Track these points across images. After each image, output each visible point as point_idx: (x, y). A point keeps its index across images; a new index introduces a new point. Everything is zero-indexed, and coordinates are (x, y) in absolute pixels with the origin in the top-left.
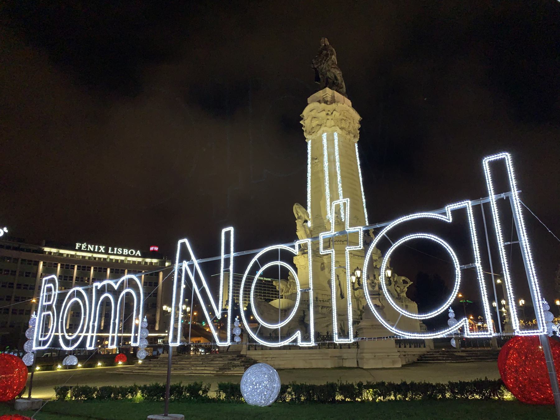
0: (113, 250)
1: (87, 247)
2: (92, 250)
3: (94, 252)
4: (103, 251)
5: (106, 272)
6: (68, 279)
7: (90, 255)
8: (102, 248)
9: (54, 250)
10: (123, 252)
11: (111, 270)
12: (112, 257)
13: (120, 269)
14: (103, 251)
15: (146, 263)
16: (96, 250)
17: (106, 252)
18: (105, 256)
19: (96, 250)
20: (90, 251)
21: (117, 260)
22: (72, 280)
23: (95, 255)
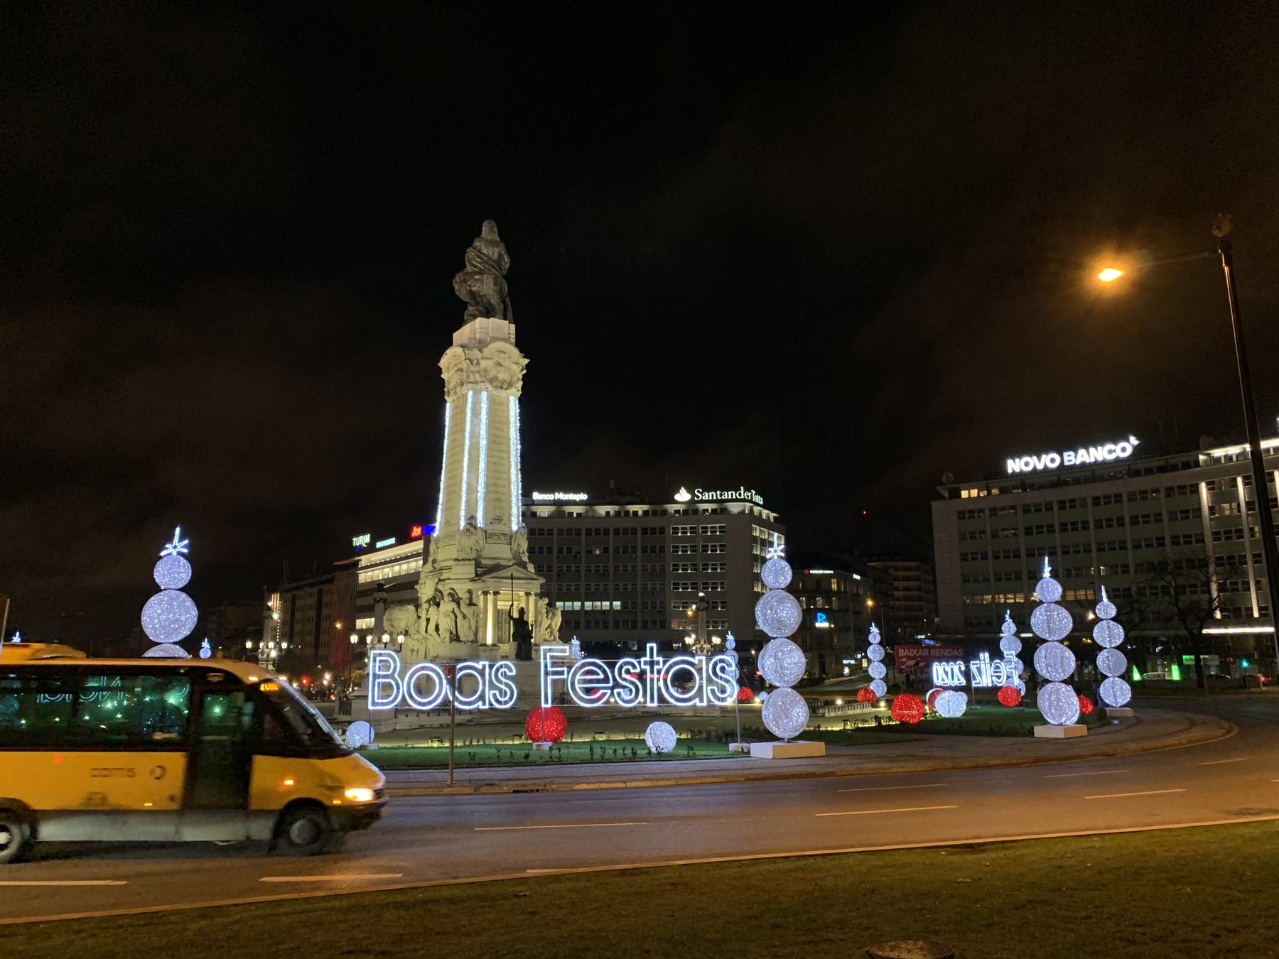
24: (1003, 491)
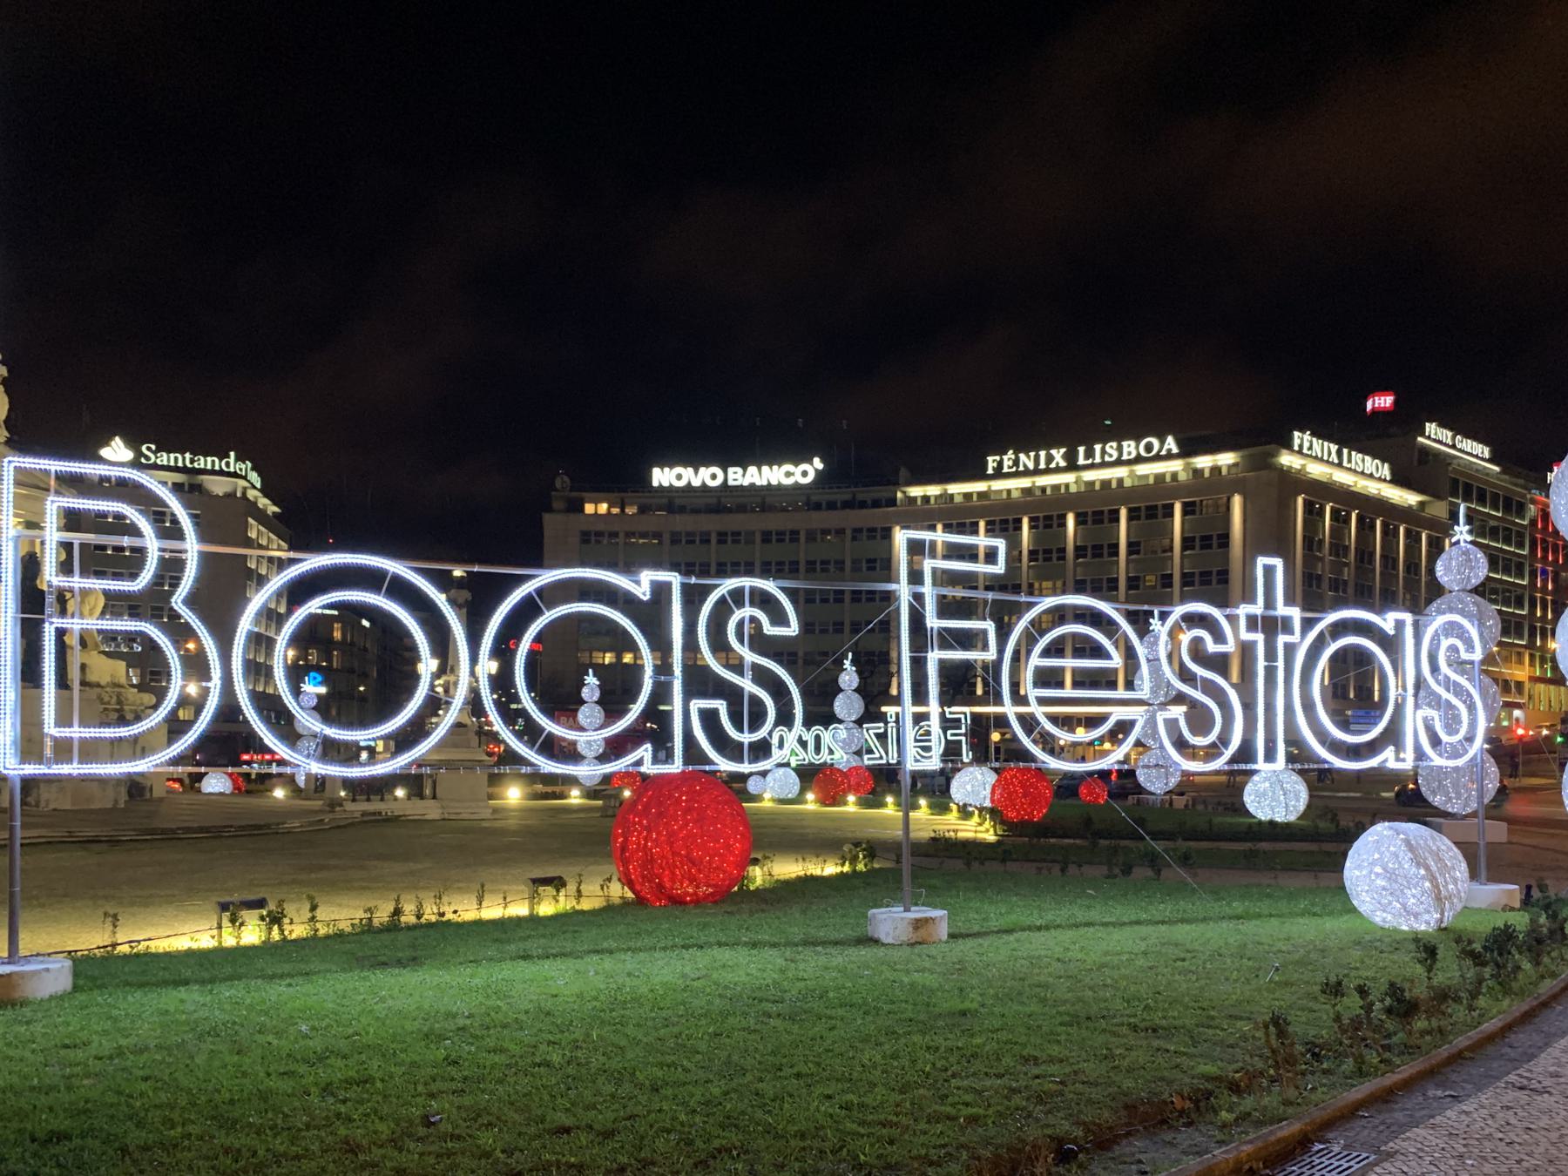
0: (1090, 454)
1: (1016, 462)
2: (1031, 466)
3: (1037, 472)
4: (1063, 464)
5: (1063, 525)
6: (1055, 556)
7: (1025, 482)
8: (1058, 455)
9: (933, 490)
10: (1121, 454)
11: (1077, 516)
12: (1088, 476)
13: (1090, 511)
14: (1063, 464)
15: (1197, 473)
16: (1042, 466)
17: (1072, 466)
18: (1069, 478)
19: (1042, 466)
20: (1027, 473)
21: (1106, 484)
22: (1117, 554)
23: (1042, 481)
24: (643, 510)
